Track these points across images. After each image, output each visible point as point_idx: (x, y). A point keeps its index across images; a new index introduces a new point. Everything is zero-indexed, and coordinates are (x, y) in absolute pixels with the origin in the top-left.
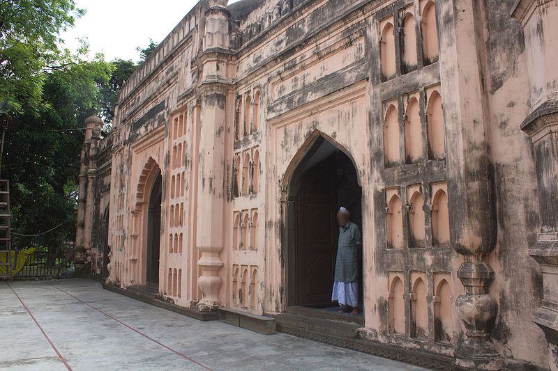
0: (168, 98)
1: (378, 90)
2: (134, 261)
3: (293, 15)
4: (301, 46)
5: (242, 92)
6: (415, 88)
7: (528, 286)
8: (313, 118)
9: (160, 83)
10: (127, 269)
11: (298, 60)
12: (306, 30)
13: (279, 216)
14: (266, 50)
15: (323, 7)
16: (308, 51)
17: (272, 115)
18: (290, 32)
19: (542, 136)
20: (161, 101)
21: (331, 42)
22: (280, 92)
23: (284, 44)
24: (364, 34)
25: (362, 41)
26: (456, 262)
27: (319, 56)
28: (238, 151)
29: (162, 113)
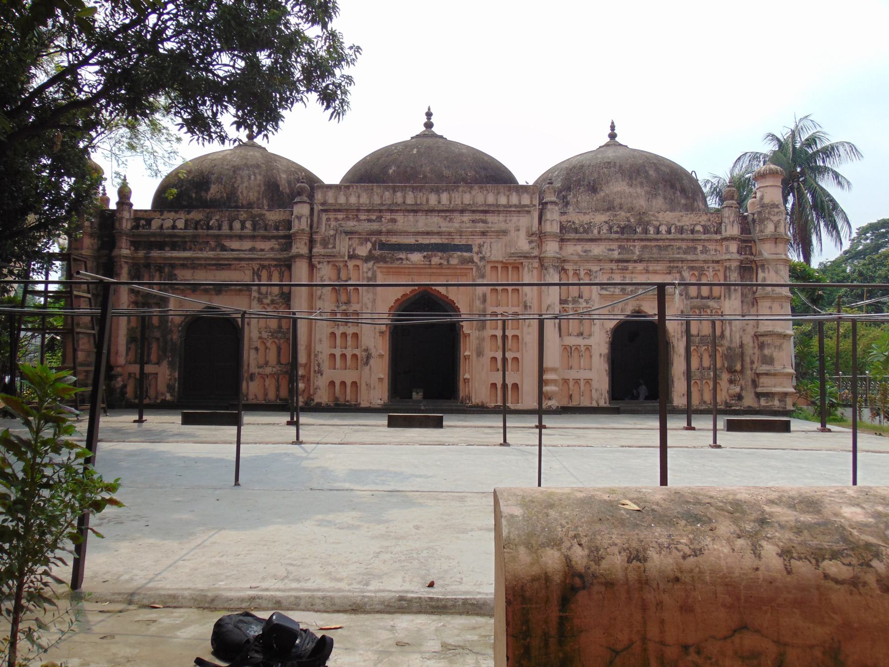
0: (480, 246)
1: (688, 302)
2: (381, 379)
3: (628, 240)
4: (635, 261)
5: (569, 267)
6: (709, 307)
7: (750, 382)
8: (638, 302)
9: (457, 225)
10: (374, 388)
11: (630, 268)
12: (638, 253)
13: (607, 351)
14: (597, 250)
15: (652, 247)
16: (640, 267)
17: (604, 292)
18: (620, 247)
19: (768, 340)
20: (464, 242)
21: (658, 268)
22: (608, 279)
23: (616, 253)
24: (680, 272)
25: (678, 275)
26: (725, 376)
27: (647, 271)
28: (565, 306)
29: (465, 254)
